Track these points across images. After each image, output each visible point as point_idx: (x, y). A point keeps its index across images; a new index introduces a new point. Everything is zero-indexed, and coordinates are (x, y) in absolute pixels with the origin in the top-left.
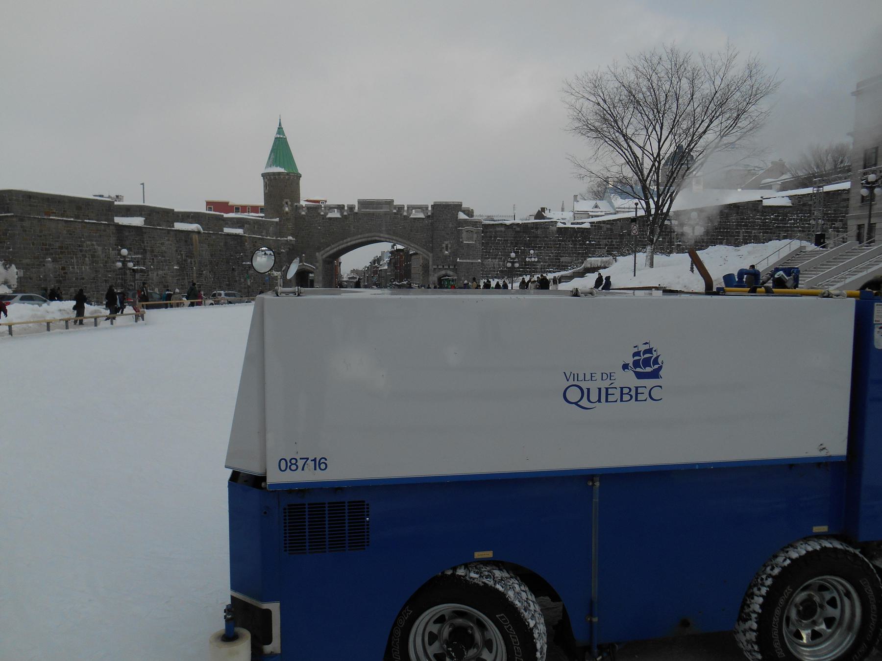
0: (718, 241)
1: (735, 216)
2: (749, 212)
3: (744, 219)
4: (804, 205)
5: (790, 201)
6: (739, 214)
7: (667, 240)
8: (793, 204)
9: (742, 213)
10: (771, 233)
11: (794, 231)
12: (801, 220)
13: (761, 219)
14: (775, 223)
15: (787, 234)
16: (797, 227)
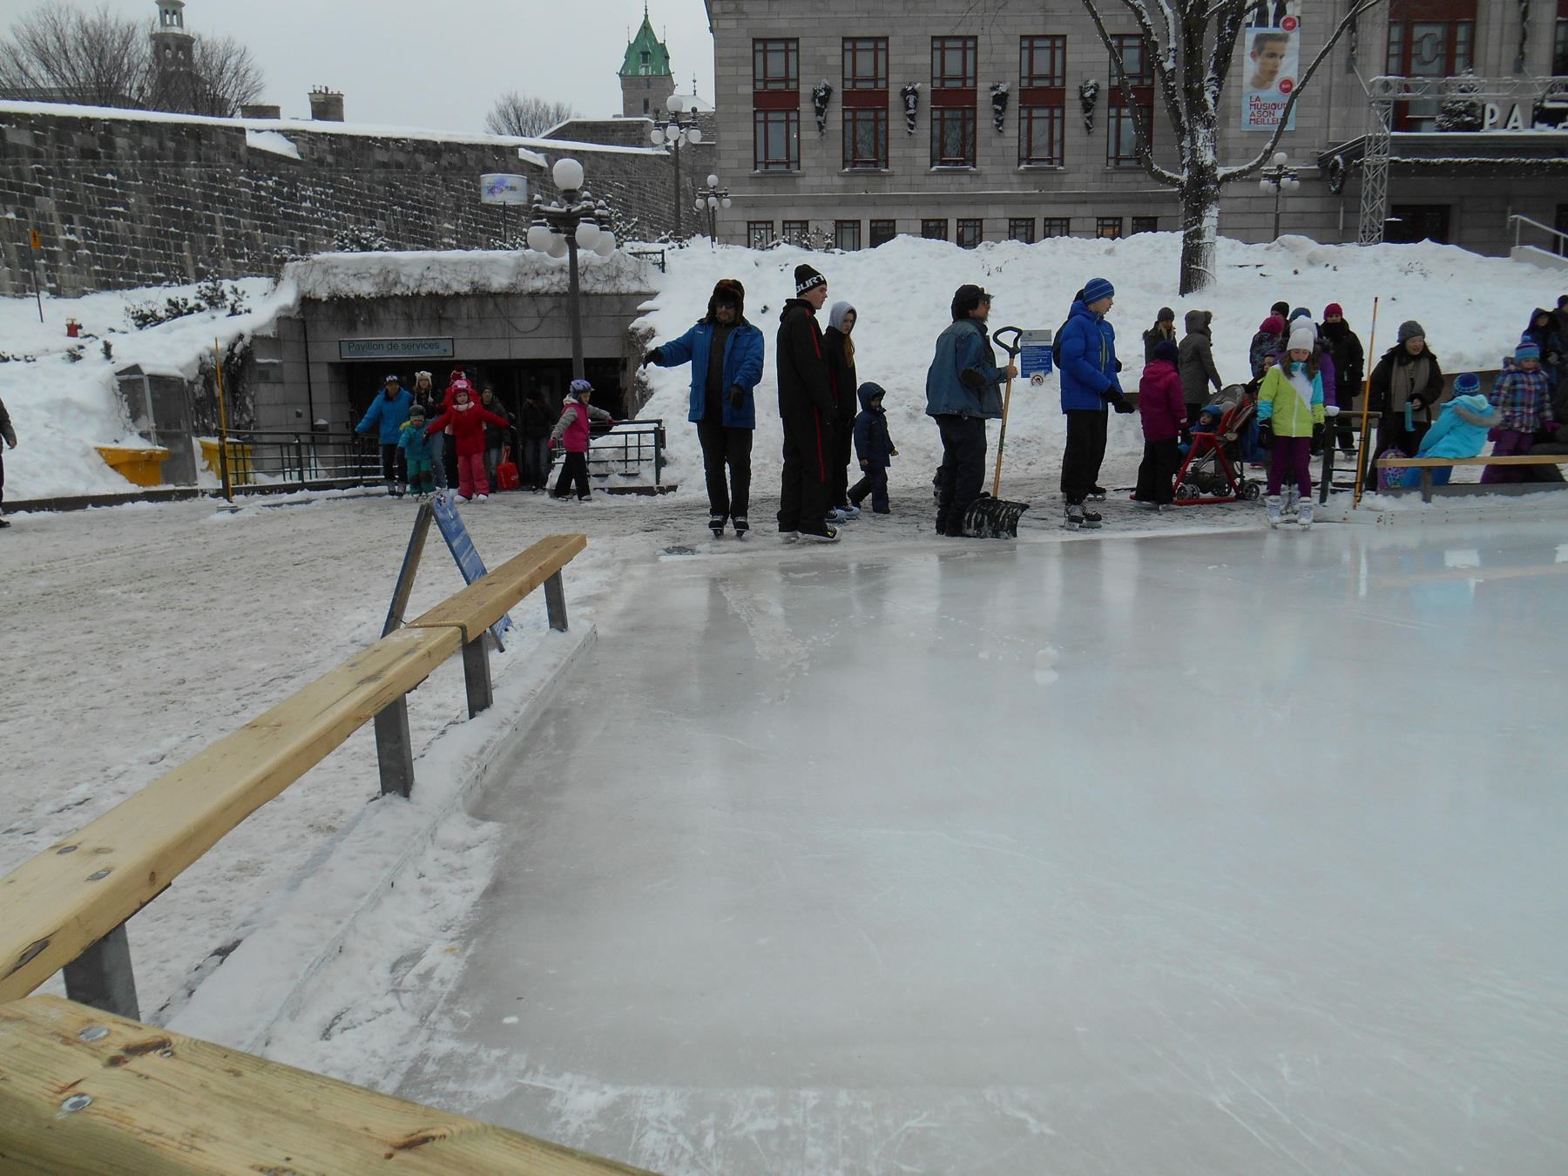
0: (172, 242)
1: (195, 166)
2: (223, 161)
3: (212, 178)
4: (321, 162)
5: (293, 145)
6: (203, 162)
7: (30, 220)
8: (302, 156)
9: (208, 159)
10: (276, 232)
11: (314, 231)
12: (321, 201)
13: (248, 185)
14: (279, 205)
15: (306, 238)
16: (318, 221)
